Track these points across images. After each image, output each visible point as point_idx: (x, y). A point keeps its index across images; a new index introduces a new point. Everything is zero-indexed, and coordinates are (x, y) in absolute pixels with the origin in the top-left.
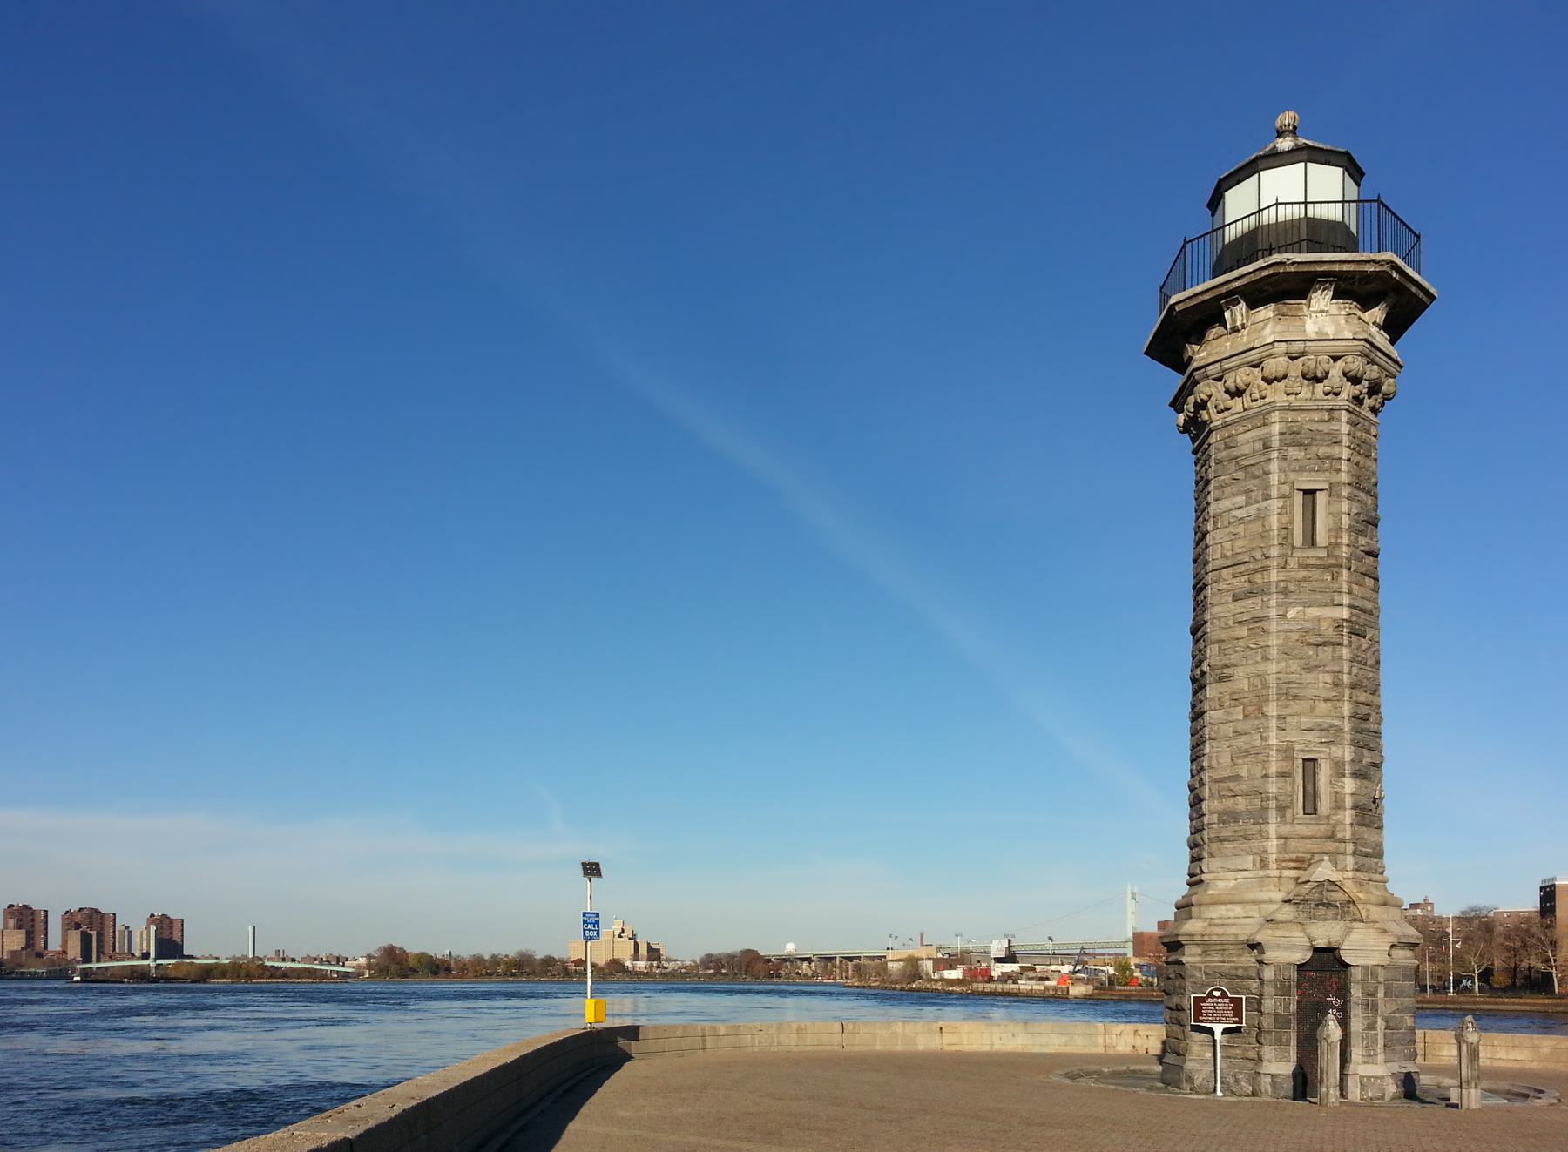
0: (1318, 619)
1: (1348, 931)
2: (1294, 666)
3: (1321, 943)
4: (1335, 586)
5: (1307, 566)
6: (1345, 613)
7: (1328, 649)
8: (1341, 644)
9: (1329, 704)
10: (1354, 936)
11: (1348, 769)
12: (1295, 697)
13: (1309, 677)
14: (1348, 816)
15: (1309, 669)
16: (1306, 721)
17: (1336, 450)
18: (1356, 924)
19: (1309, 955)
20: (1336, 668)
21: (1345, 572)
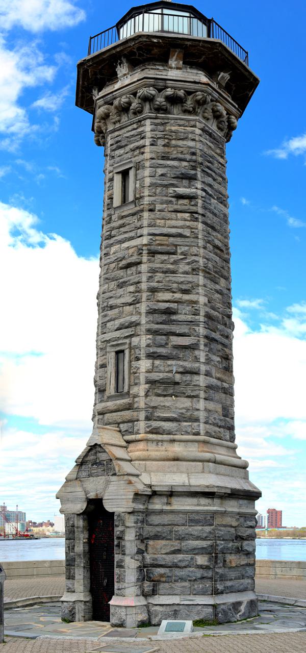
0: (128, 248)
1: (108, 483)
2: (113, 285)
3: (92, 495)
4: (138, 225)
5: (123, 217)
6: (145, 240)
7: (134, 269)
8: (140, 263)
9: (132, 306)
10: (112, 488)
11: (142, 354)
12: (112, 307)
13: (120, 291)
14: (141, 389)
15: (121, 286)
16: (117, 323)
17: (141, 142)
18: (114, 478)
19: (84, 506)
20: (136, 280)
21: (146, 214)
